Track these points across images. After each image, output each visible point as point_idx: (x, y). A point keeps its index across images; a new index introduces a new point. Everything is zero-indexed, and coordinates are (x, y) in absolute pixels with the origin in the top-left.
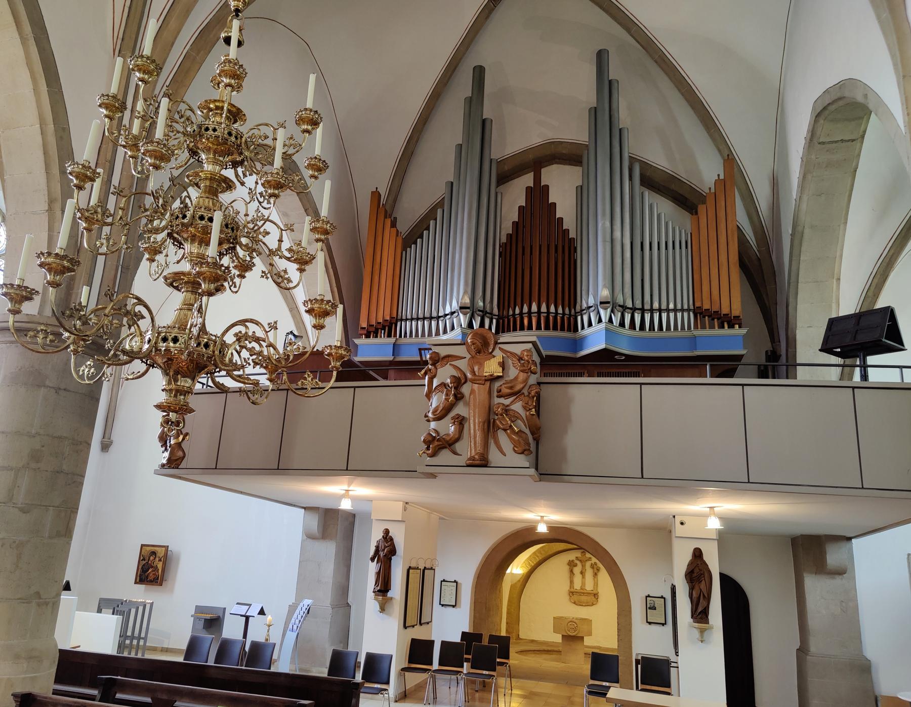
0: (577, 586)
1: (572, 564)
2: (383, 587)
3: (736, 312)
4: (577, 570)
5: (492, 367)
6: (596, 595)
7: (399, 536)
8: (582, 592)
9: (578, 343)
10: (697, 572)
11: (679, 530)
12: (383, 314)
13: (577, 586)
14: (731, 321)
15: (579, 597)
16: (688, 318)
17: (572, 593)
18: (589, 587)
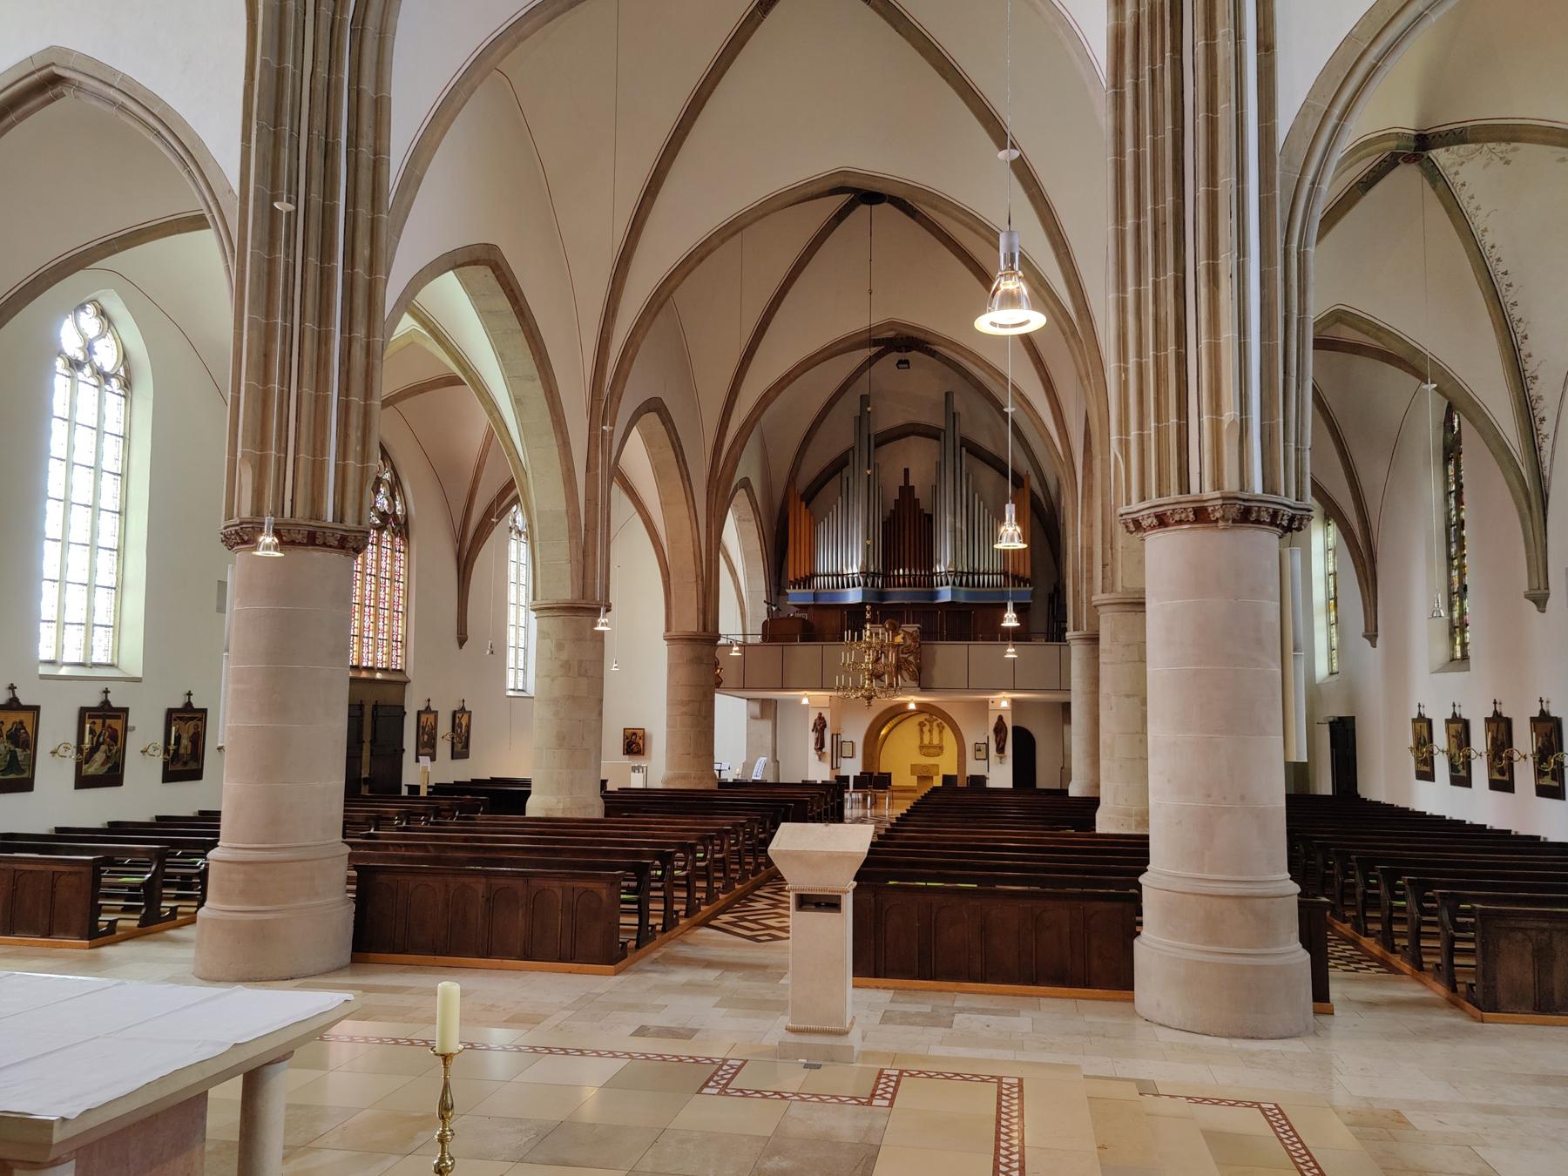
0: (926, 742)
1: (921, 725)
2: (820, 745)
3: (1028, 574)
4: (926, 729)
5: (899, 639)
6: (941, 748)
7: (827, 716)
8: (930, 746)
9: (935, 595)
10: (1000, 728)
11: (991, 706)
12: (804, 572)
13: (926, 742)
14: (1026, 581)
15: (925, 749)
16: (1000, 579)
17: (922, 747)
18: (936, 742)
